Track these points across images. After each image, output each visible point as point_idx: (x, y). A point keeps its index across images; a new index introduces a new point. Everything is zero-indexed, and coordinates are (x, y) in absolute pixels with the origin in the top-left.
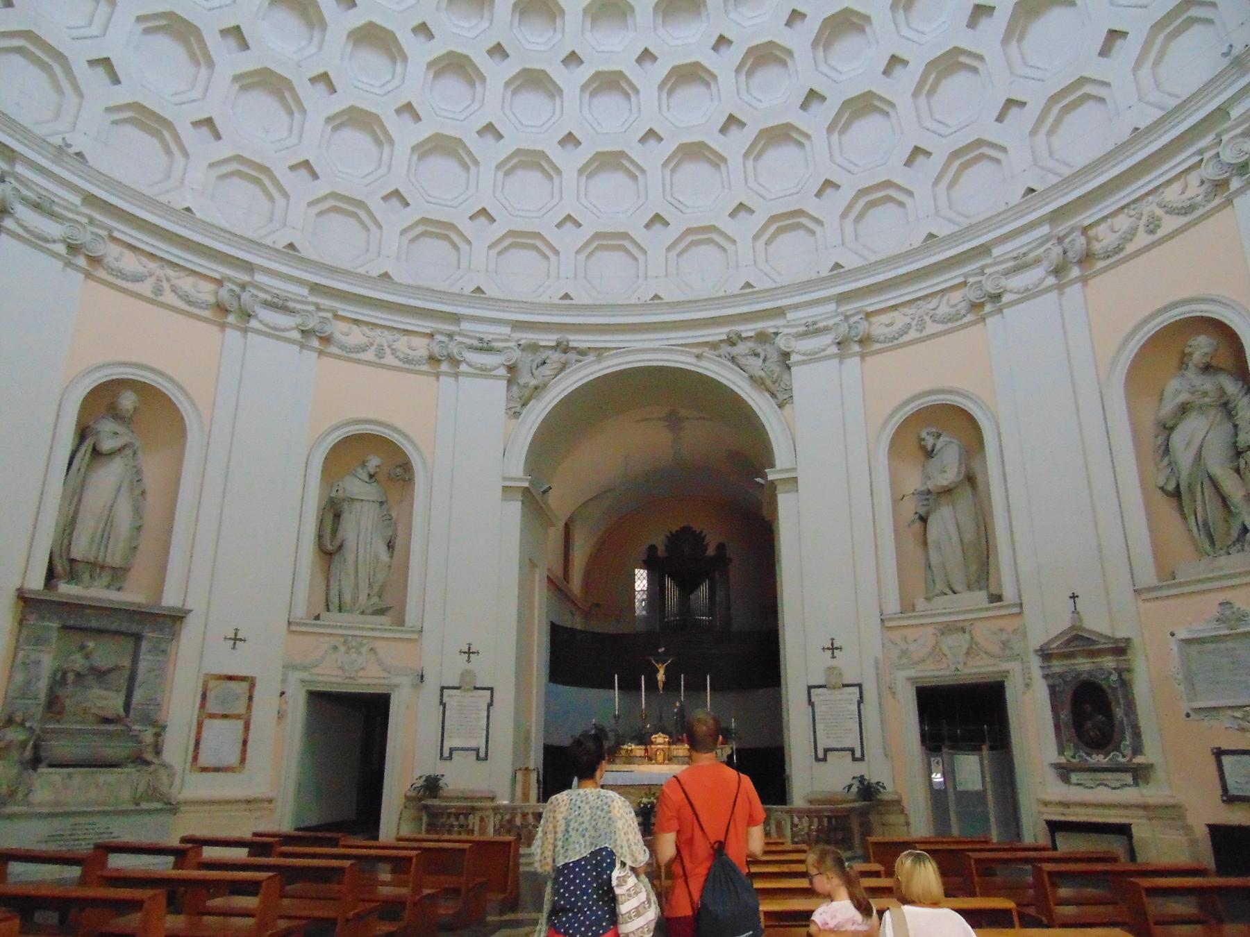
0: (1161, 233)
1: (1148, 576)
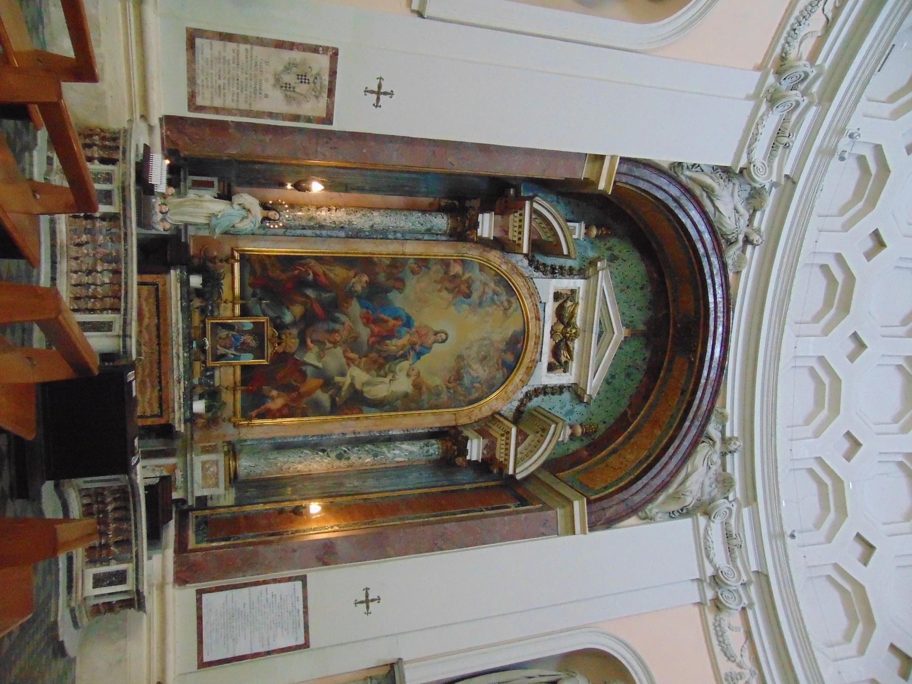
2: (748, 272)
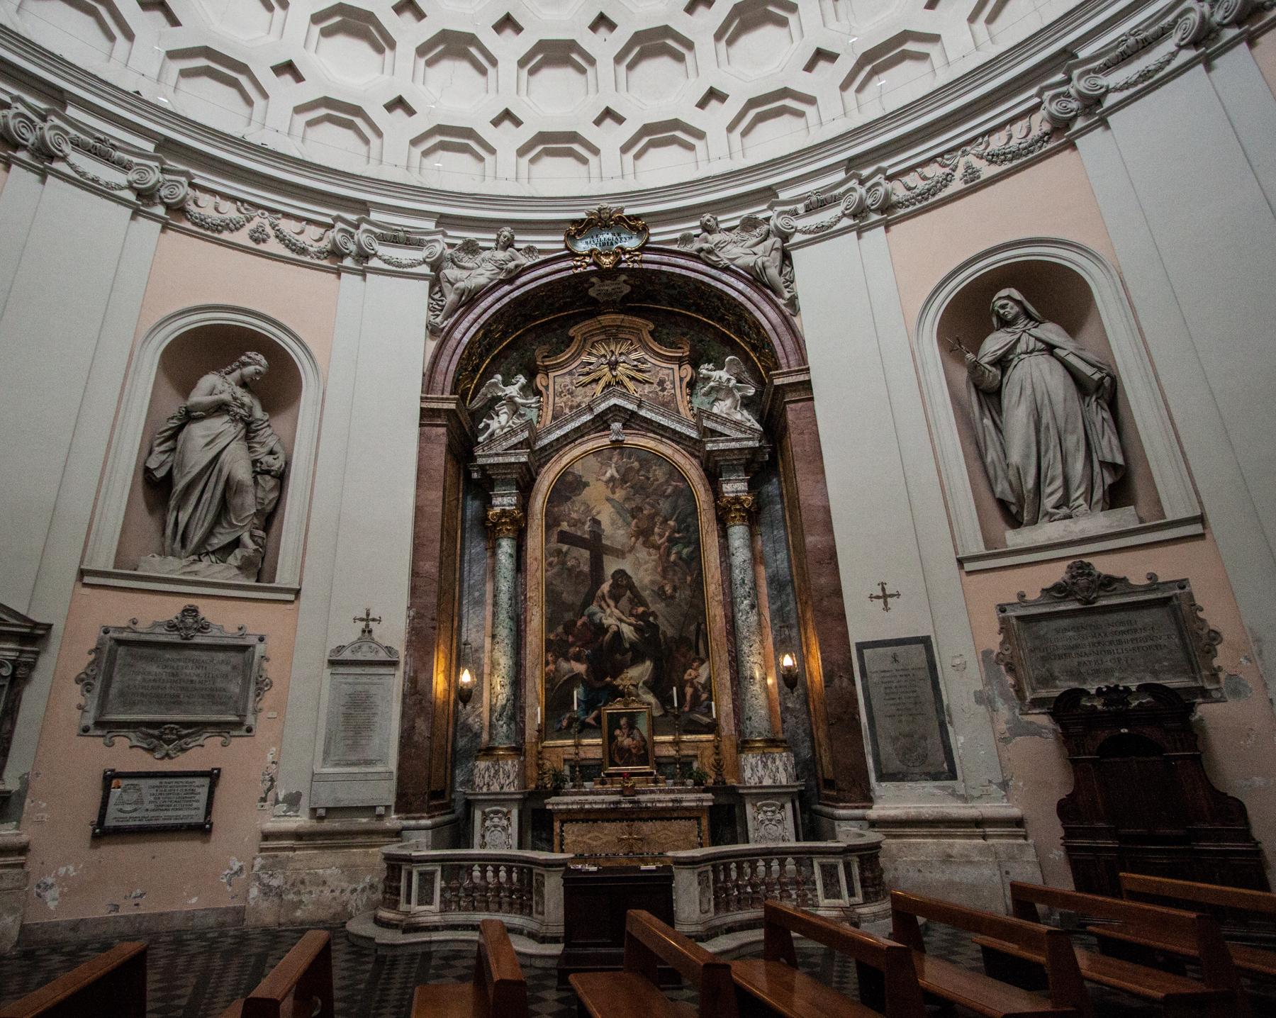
0: (262, 247)
1: (103, 559)
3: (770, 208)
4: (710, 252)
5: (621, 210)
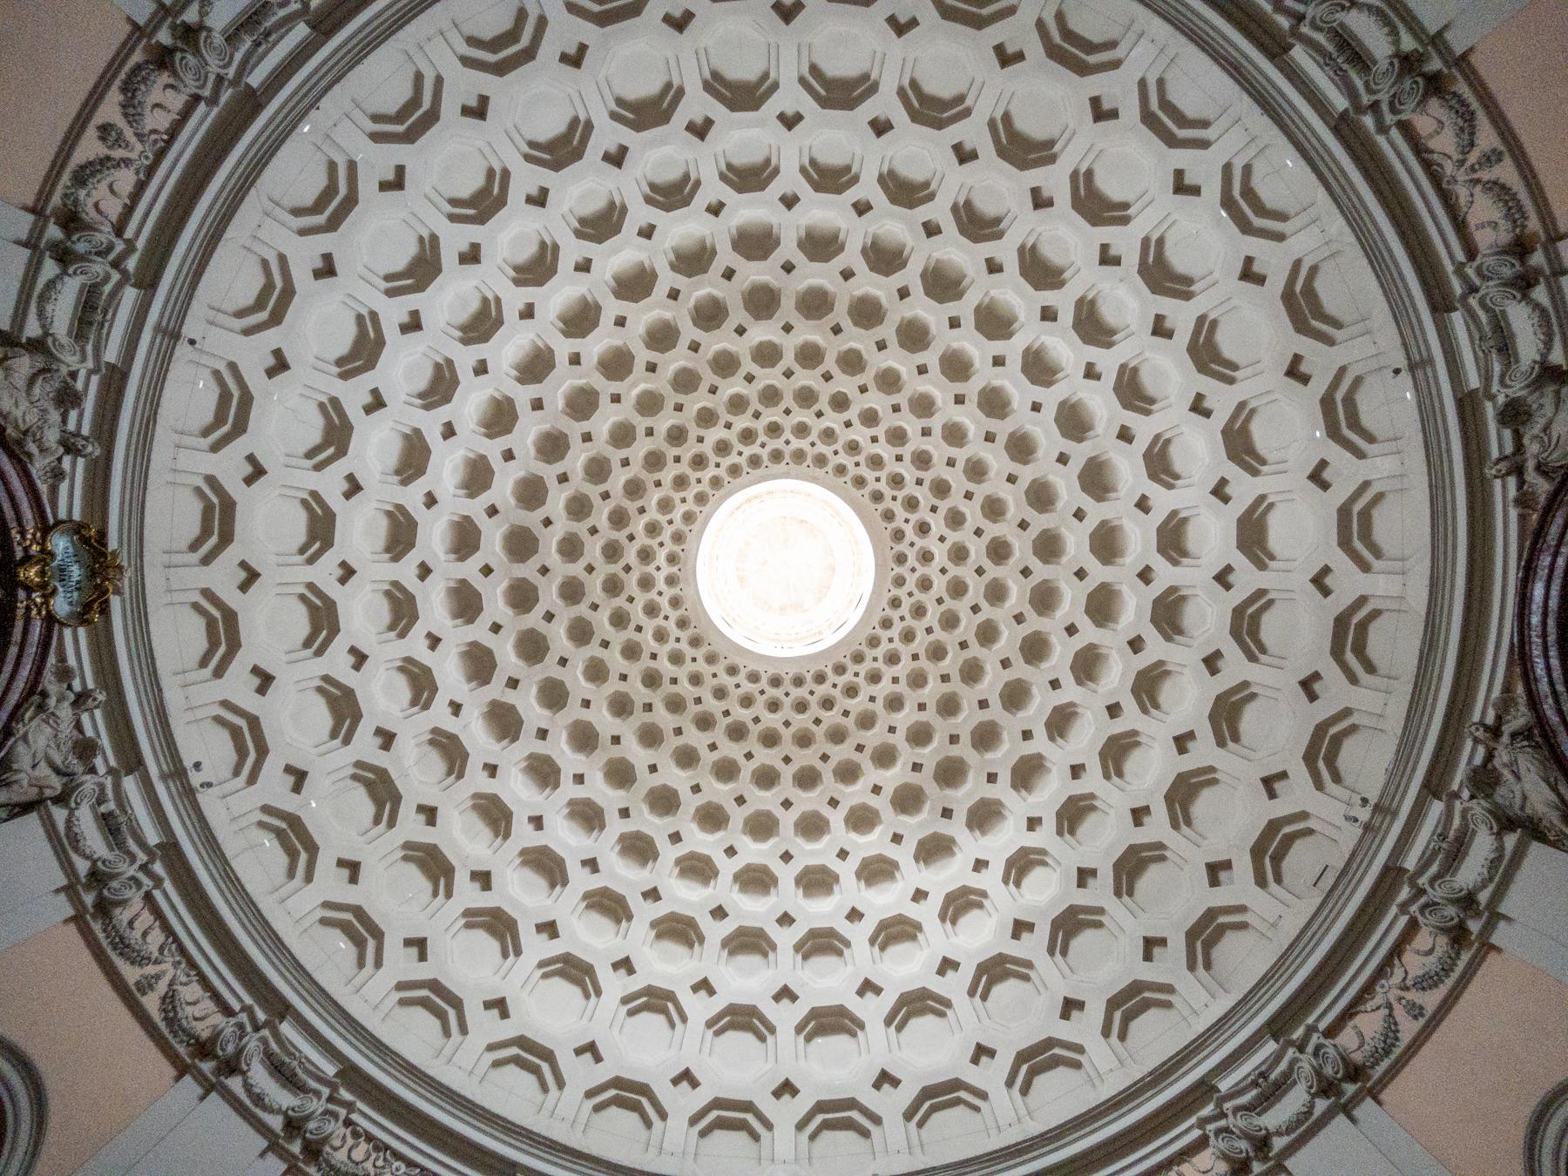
2: (1489, 690)
3: (111, 771)
4: (41, 708)
5: (118, 592)
